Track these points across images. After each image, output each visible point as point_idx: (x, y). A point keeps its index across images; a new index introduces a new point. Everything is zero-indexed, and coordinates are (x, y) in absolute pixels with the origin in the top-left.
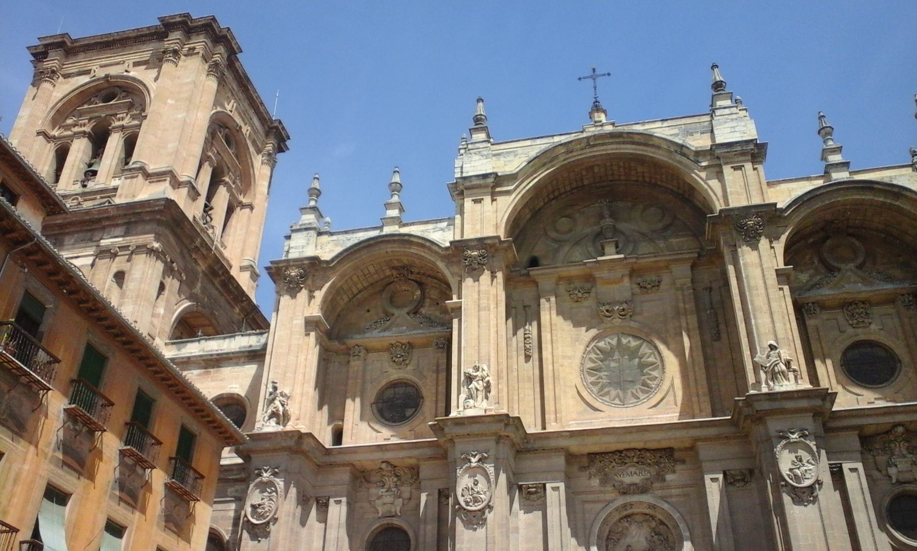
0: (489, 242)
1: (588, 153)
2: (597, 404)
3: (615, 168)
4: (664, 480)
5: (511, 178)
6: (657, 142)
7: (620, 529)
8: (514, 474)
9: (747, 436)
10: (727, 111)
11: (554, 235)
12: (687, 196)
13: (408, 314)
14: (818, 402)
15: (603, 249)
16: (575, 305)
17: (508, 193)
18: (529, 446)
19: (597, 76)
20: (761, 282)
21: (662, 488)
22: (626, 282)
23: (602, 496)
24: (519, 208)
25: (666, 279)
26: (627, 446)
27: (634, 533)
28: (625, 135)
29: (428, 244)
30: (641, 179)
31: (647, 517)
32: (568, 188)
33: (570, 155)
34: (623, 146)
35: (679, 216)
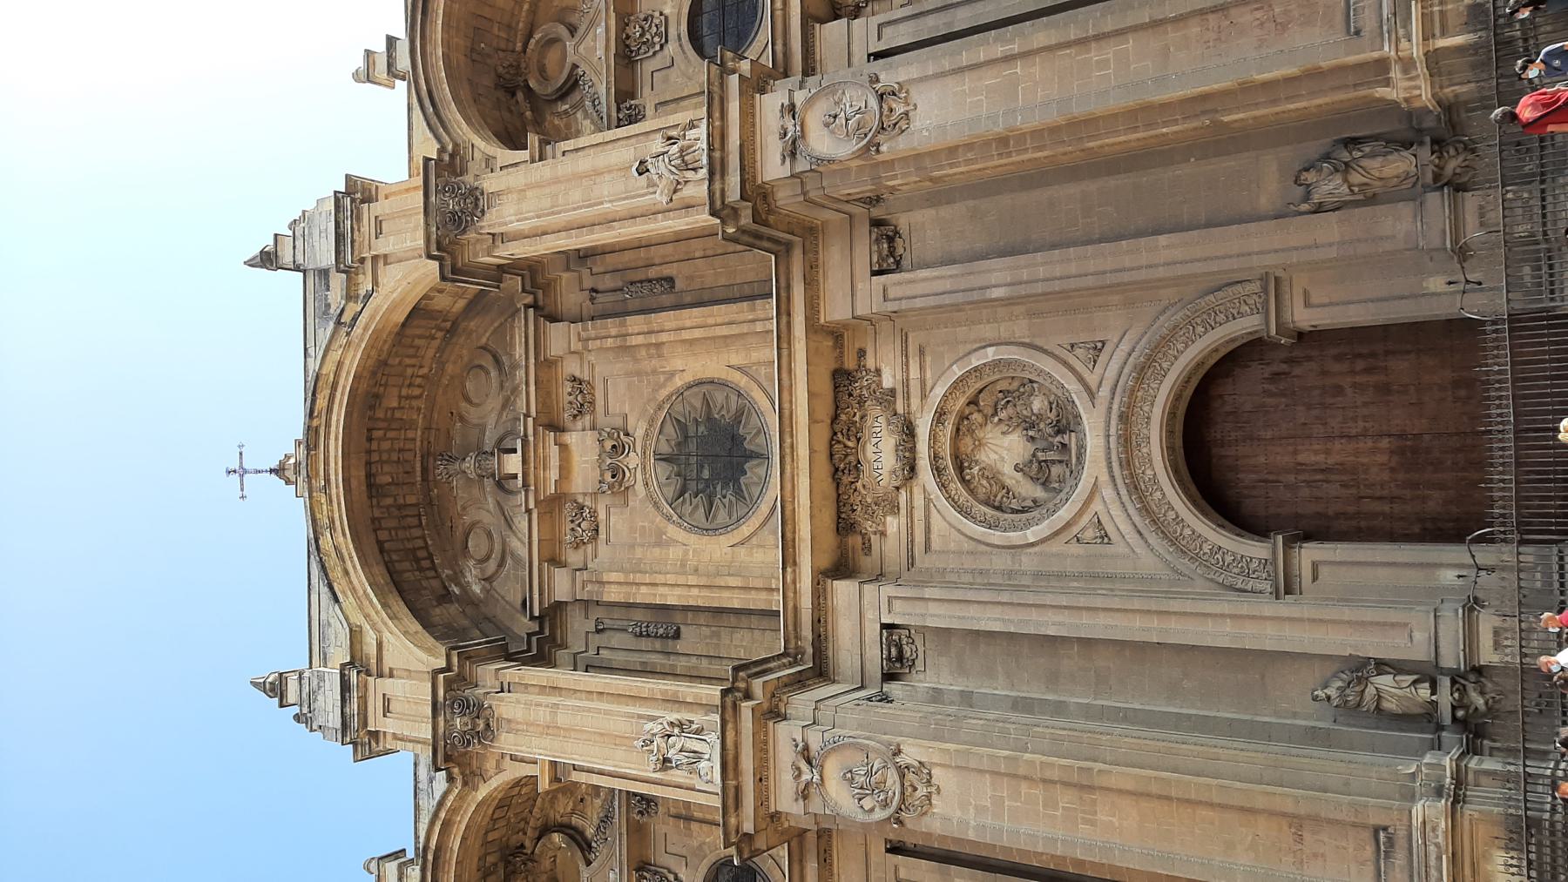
0: (441, 692)
1: (338, 489)
2: (764, 508)
3: (386, 445)
4: (893, 392)
5: (355, 635)
6: (329, 368)
7: (984, 482)
8: (862, 687)
9: (811, 229)
10: (299, 243)
11: (492, 566)
12: (448, 324)
13: (589, 863)
14: (734, 80)
15: (515, 476)
16: (602, 536)
17: (380, 646)
18: (810, 650)
19: (241, 466)
20: (547, 190)
21: (907, 396)
22: (571, 438)
23: (919, 514)
24: (415, 626)
25: (572, 367)
26: (822, 457)
27: (993, 456)
28: (315, 423)
29: (442, 815)
30: (415, 403)
31: (963, 429)
32: (416, 532)
33: (338, 523)
34: (333, 428)
35: (484, 340)
